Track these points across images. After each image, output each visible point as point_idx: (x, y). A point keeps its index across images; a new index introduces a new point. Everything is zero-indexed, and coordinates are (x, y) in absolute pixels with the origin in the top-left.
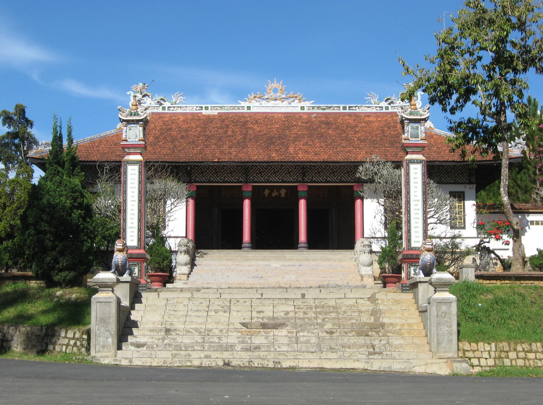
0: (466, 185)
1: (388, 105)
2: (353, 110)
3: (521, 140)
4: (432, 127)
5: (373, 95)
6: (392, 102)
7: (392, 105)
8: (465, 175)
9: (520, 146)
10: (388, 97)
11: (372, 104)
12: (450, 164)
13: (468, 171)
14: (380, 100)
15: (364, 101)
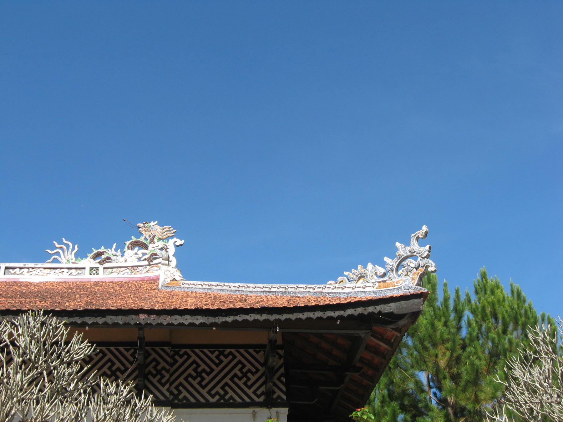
0: (257, 409)
1: (98, 265)
2: (14, 273)
3: (415, 246)
4: (178, 278)
5: (67, 246)
6: (108, 259)
7: (107, 265)
8: (253, 378)
9: (412, 263)
10: (103, 249)
11: (60, 262)
12: (187, 320)
13: (262, 369)
14: (81, 255)
15: (44, 258)
